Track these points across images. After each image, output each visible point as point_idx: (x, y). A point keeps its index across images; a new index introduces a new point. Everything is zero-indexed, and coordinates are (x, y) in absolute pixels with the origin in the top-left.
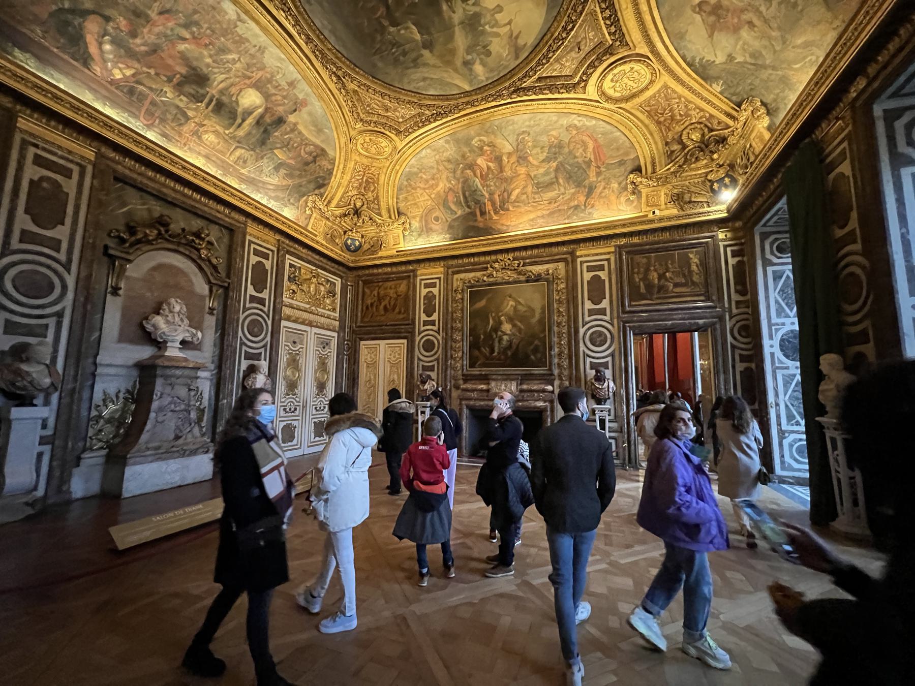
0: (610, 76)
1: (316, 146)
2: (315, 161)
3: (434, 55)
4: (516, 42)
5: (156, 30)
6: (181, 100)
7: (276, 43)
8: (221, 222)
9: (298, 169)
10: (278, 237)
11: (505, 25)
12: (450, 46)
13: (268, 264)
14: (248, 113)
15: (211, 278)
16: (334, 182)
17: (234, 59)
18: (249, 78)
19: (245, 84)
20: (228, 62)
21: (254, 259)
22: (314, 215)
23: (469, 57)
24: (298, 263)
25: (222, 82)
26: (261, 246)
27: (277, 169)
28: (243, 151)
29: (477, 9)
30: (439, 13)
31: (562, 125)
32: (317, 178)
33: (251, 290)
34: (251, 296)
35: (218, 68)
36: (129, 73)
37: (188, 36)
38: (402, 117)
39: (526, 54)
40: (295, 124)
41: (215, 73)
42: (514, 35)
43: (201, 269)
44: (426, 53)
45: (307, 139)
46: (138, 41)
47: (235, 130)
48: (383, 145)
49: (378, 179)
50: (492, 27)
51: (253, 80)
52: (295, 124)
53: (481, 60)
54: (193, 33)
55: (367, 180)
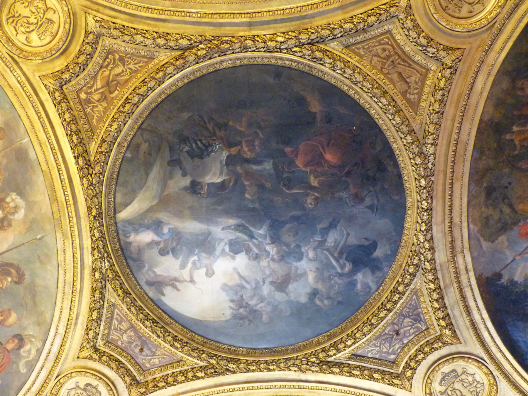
0: (95, 382)
3: (180, 190)
4: (169, 285)
11: (191, 277)
12: (187, 212)
23: (166, 230)
29: (218, 252)
30: (227, 213)
31: (25, 329)
38: (88, 101)
39: (151, 294)
42: (177, 284)
44: (186, 182)
48: (34, 36)
50: (194, 263)
53: (157, 243)
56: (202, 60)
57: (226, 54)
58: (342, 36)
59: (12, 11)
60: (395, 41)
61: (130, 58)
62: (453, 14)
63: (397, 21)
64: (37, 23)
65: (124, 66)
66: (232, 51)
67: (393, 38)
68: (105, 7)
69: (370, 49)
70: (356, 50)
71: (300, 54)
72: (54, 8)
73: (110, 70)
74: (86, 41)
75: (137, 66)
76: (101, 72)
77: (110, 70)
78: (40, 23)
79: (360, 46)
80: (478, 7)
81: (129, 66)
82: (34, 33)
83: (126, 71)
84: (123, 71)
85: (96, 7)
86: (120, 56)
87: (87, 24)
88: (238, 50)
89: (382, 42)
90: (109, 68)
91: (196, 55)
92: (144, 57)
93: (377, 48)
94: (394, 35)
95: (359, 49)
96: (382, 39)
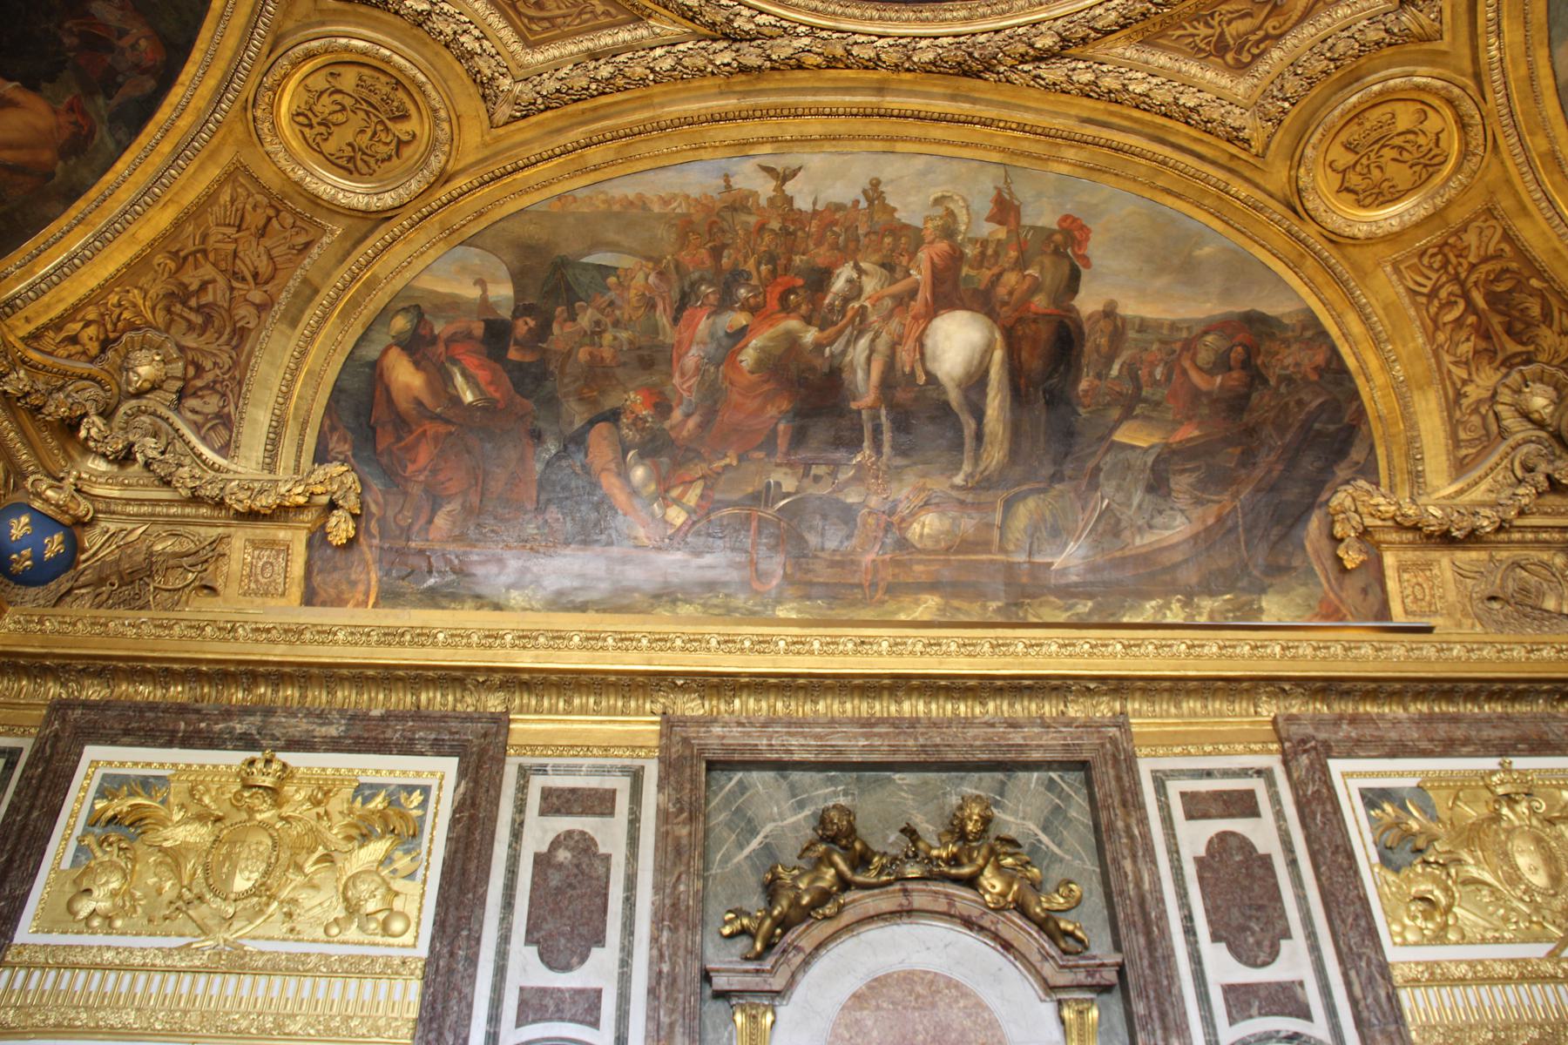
1: (1221, 326)
2: (1255, 377)
5: (692, 357)
6: (817, 479)
7: (879, 146)
8: (1036, 756)
9: (1227, 441)
10: (1269, 709)
13: (1261, 833)
14: (976, 382)
15: (1048, 969)
16: (1375, 394)
17: (850, 281)
18: (913, 294)
19: (915, 318)
20: (846, 300)
21: (1196, 837)
22: (1389, 559)
24: (1402, 772)
25: (869, 360)
26: (1209, 774)
27: (1158, 485)
28: (1031, 503)
32: (1306, 427)
33: (1223, 967)
34: (1229, 990)
35: (840, 333)
36: (692, 497)
37: (742, 319)
40: (1109, 313)
41: (844, 353)
43: (1007, 946)
45: (1174, 326)
46: (677, 415)
47: (977, 459)
48: (1402, 125)
49: (1522, 254)
51: (924, 294)
52: (1109, 313)
54: (746, 307)
55: (1492, 298)
56: (1021, 31)
57: (955, 36)
58: (652, 49)
59: (1424, 176)
60: (511, 23)
61: (1200, 50)
62: (376, 74)
63: (514, 72)
64: (1383, 146)
65: (1222, 34)
66: (938, 42)
67: (517, 31)
68: (1213, 163)
69: (576, 10)
70: (613, 11)
71: (762, 19)
72: (1329, 171)
73: (1260, 28)
74: (1286, 105)
75: (1191, 30)
76: (1285, 28)
77: (1260, 28)
78: (1377, 147)
79: (603, 20)
80: (319, 82)
81: (1210, 31)
82: (1401, 127)
83: (1220, 23)
84: (1229, 23)
85: (1232, 164)
86: (1223, 57)
87: (1270, 137)
88: (924, 43)
89: (547, 24)
90: (1261, 33)
91: (1031, 46)
92: (1164, 49)
93: (557, 12)
94: (516, 38)
95: (607, 13)
96: (545, 30)
